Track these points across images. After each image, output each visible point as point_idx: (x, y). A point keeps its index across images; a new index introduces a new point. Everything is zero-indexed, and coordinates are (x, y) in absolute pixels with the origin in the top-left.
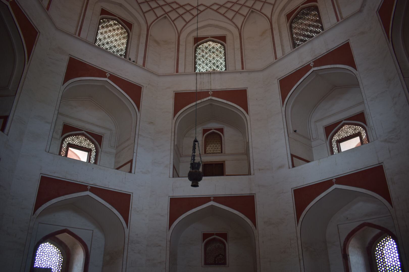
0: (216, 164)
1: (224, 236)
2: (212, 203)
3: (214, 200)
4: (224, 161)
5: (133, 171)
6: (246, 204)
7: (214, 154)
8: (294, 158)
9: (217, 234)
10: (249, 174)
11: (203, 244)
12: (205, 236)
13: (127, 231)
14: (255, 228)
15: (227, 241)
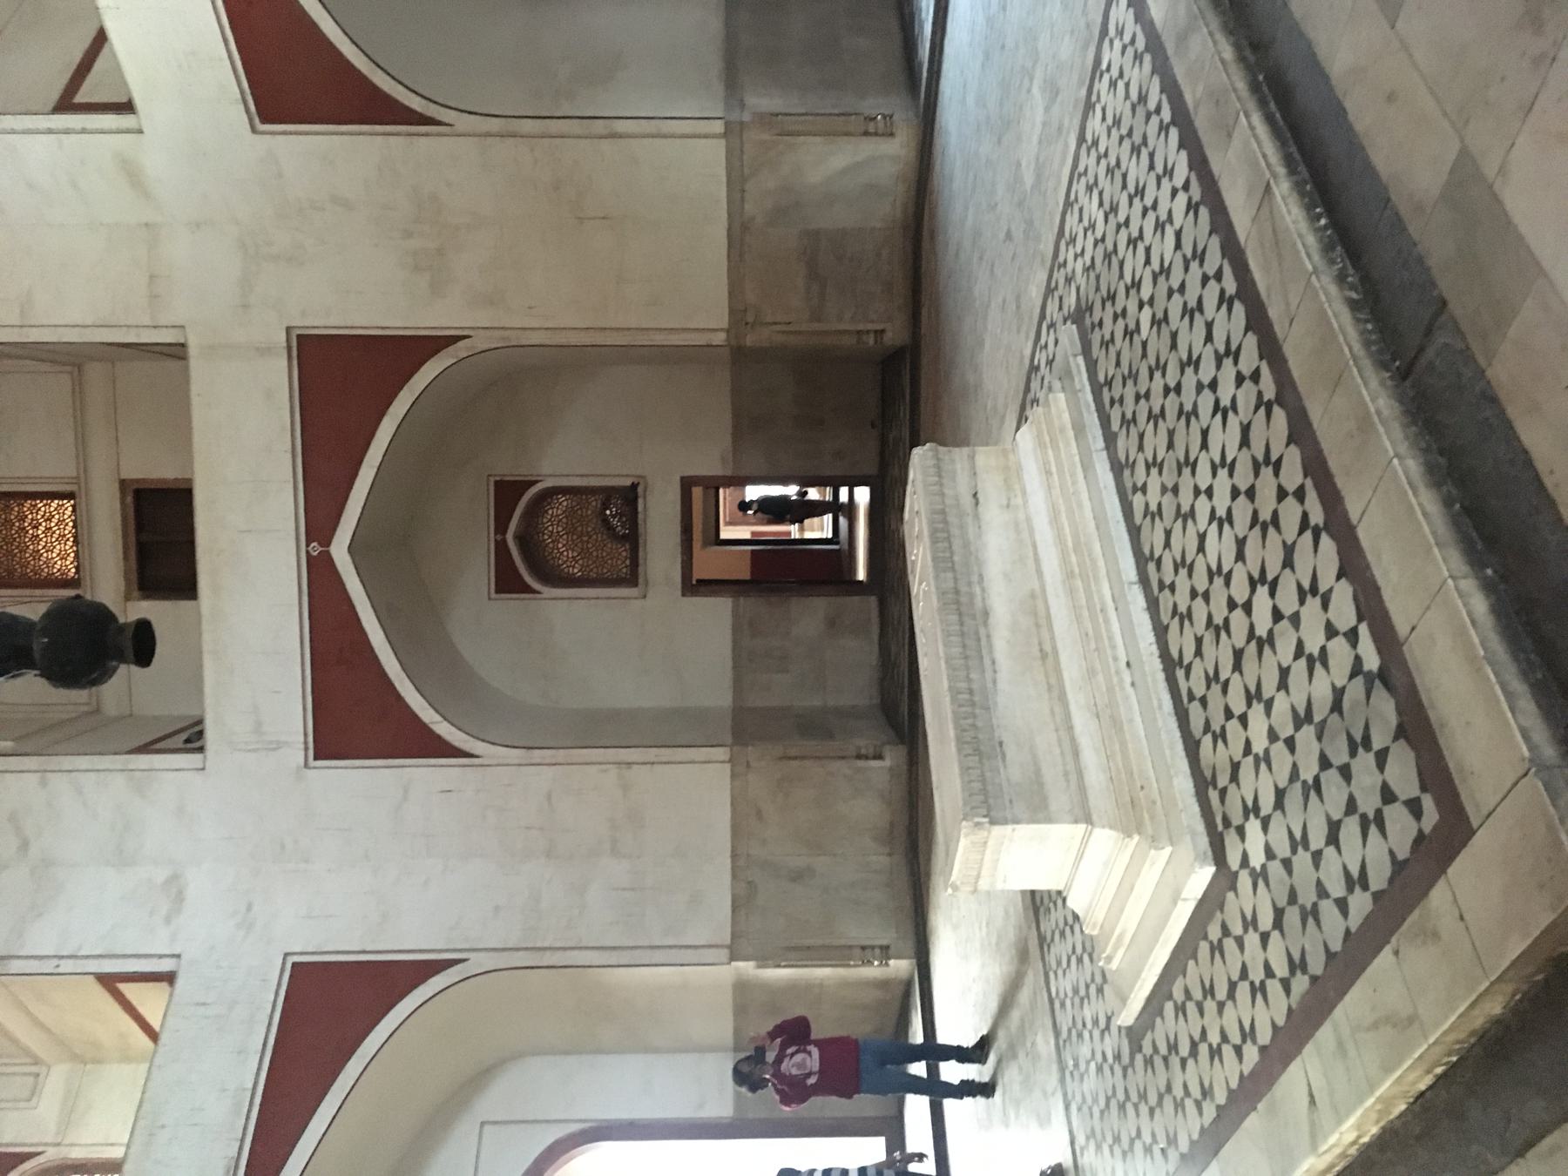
0: (140, 528)
1: (507, 492)
2: (340, 551)
3: (327, 541)
4: (123, 483)
5: (164, 966)
6: (341, 381)
7: (84, 538)
8: (79, 98)
9: (501, 527)
10: (177, 352)
11: (548, 592)
12: (508, 582)
13: (478, 962)
14: (461, 344)
15: (534, 483)
